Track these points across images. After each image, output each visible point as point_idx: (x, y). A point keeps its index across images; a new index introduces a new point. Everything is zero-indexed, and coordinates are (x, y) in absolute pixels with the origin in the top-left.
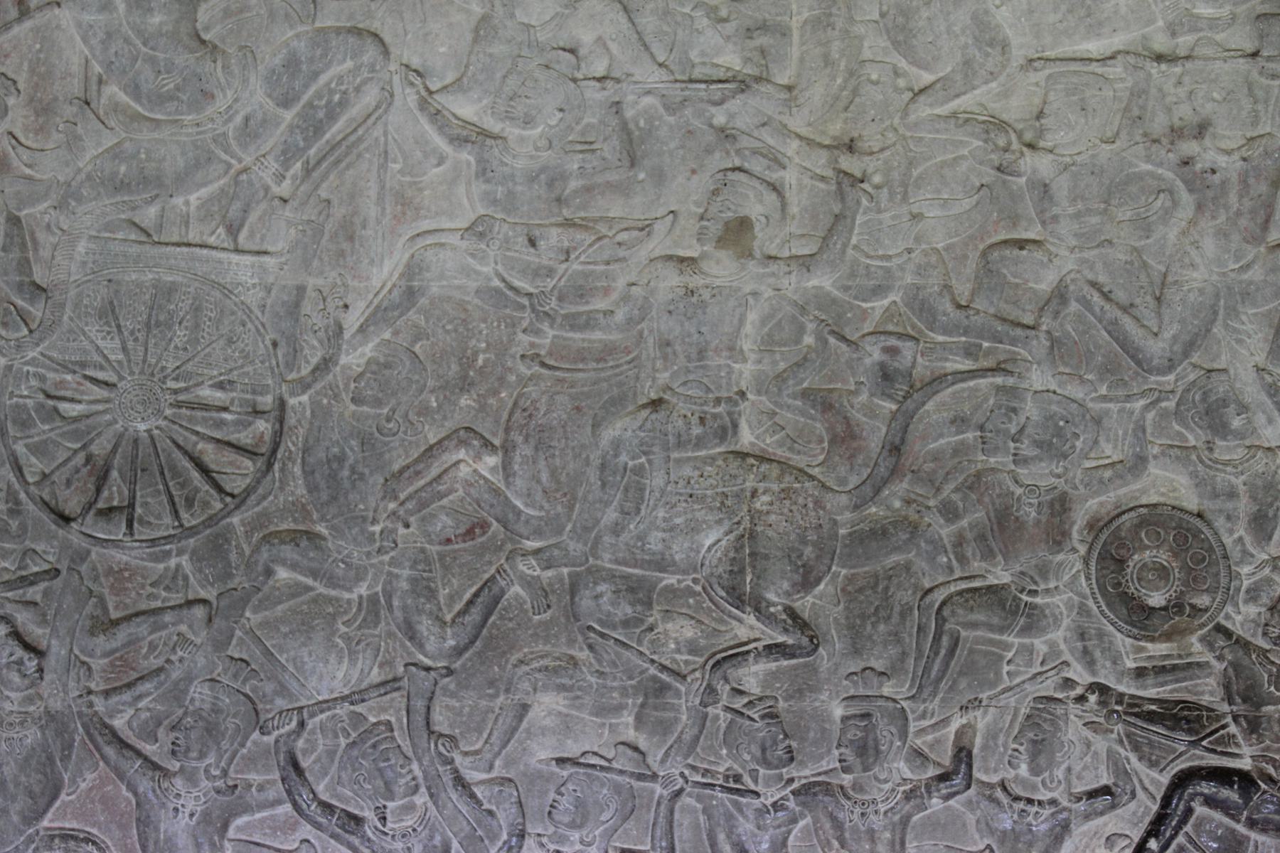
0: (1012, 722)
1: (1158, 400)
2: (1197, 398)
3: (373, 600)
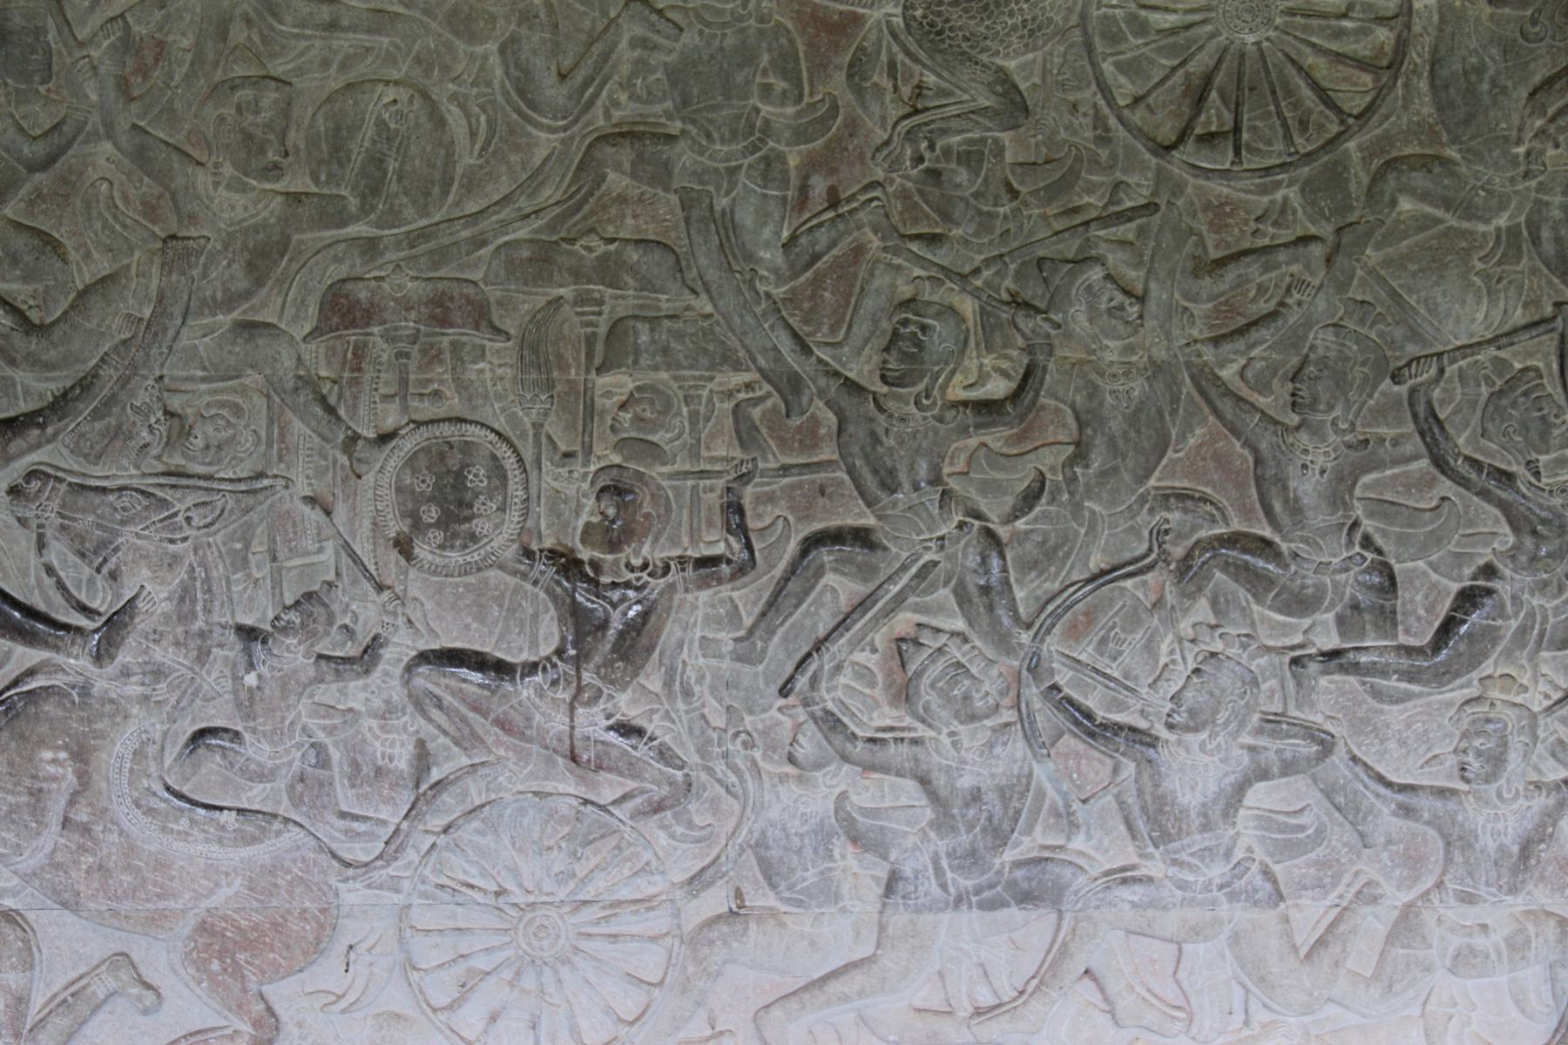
3: (1513, 231)
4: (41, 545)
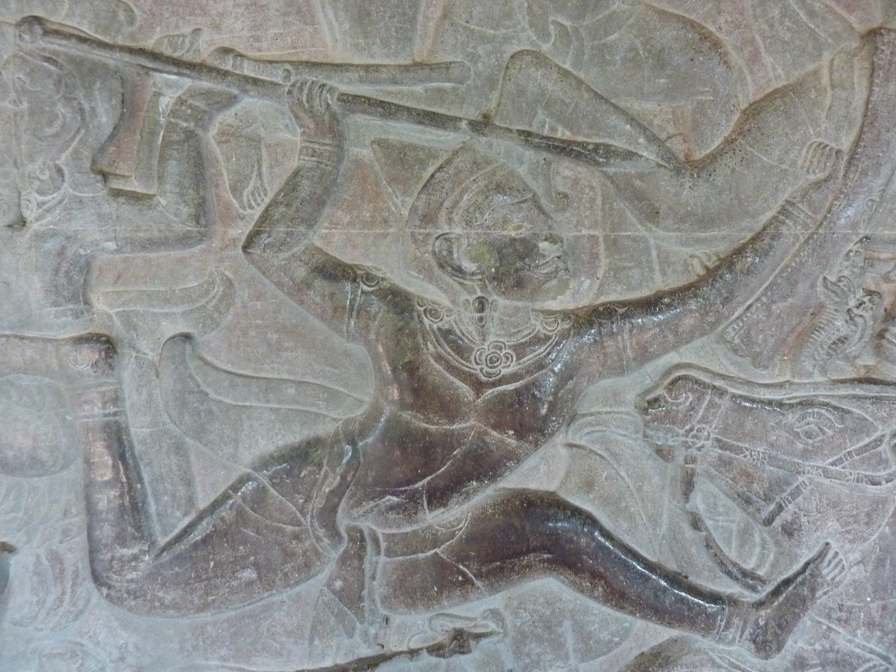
4: (688, 485)
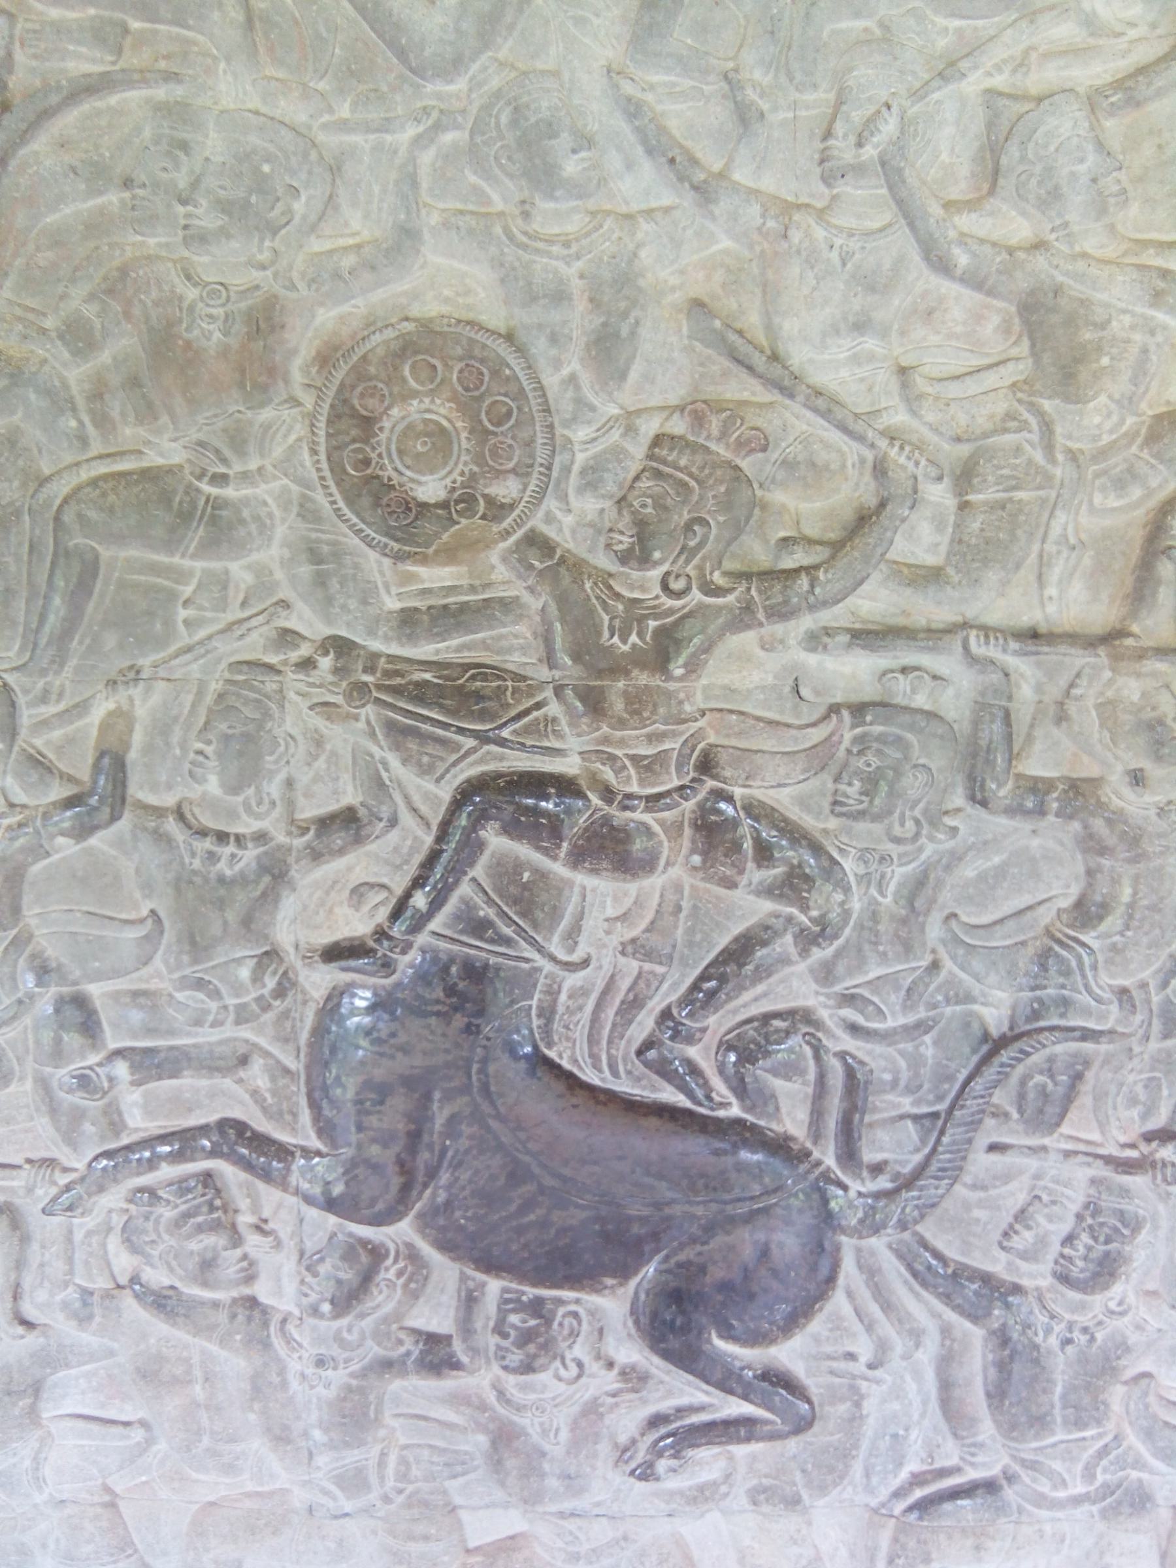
0: (194, 706)
1: (437, 127)
2: (504, 119)
